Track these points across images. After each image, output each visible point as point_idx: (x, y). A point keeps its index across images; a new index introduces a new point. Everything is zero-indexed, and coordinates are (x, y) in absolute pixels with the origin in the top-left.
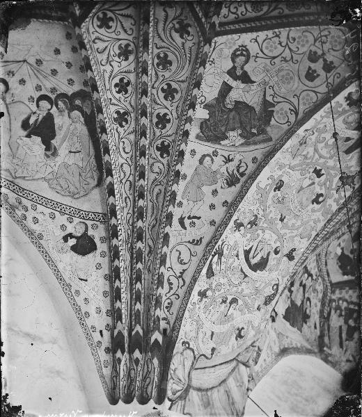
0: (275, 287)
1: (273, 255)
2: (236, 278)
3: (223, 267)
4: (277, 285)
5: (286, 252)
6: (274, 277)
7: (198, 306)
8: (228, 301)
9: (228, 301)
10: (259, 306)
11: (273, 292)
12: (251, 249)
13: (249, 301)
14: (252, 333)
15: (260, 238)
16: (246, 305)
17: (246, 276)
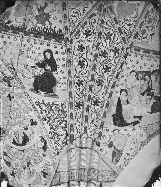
0: (42, 140)
1: (26, 132)
2: (21, 155)
3: (11, 157)
4: (43, 138)
7: (14, 180)
8: (26, 166)
9: (26, 166)
10: (43, 154)
11: (44, 143)
12: (14, 140)
14: (52, 167)
15: (13, 133)
17: (23, 150)
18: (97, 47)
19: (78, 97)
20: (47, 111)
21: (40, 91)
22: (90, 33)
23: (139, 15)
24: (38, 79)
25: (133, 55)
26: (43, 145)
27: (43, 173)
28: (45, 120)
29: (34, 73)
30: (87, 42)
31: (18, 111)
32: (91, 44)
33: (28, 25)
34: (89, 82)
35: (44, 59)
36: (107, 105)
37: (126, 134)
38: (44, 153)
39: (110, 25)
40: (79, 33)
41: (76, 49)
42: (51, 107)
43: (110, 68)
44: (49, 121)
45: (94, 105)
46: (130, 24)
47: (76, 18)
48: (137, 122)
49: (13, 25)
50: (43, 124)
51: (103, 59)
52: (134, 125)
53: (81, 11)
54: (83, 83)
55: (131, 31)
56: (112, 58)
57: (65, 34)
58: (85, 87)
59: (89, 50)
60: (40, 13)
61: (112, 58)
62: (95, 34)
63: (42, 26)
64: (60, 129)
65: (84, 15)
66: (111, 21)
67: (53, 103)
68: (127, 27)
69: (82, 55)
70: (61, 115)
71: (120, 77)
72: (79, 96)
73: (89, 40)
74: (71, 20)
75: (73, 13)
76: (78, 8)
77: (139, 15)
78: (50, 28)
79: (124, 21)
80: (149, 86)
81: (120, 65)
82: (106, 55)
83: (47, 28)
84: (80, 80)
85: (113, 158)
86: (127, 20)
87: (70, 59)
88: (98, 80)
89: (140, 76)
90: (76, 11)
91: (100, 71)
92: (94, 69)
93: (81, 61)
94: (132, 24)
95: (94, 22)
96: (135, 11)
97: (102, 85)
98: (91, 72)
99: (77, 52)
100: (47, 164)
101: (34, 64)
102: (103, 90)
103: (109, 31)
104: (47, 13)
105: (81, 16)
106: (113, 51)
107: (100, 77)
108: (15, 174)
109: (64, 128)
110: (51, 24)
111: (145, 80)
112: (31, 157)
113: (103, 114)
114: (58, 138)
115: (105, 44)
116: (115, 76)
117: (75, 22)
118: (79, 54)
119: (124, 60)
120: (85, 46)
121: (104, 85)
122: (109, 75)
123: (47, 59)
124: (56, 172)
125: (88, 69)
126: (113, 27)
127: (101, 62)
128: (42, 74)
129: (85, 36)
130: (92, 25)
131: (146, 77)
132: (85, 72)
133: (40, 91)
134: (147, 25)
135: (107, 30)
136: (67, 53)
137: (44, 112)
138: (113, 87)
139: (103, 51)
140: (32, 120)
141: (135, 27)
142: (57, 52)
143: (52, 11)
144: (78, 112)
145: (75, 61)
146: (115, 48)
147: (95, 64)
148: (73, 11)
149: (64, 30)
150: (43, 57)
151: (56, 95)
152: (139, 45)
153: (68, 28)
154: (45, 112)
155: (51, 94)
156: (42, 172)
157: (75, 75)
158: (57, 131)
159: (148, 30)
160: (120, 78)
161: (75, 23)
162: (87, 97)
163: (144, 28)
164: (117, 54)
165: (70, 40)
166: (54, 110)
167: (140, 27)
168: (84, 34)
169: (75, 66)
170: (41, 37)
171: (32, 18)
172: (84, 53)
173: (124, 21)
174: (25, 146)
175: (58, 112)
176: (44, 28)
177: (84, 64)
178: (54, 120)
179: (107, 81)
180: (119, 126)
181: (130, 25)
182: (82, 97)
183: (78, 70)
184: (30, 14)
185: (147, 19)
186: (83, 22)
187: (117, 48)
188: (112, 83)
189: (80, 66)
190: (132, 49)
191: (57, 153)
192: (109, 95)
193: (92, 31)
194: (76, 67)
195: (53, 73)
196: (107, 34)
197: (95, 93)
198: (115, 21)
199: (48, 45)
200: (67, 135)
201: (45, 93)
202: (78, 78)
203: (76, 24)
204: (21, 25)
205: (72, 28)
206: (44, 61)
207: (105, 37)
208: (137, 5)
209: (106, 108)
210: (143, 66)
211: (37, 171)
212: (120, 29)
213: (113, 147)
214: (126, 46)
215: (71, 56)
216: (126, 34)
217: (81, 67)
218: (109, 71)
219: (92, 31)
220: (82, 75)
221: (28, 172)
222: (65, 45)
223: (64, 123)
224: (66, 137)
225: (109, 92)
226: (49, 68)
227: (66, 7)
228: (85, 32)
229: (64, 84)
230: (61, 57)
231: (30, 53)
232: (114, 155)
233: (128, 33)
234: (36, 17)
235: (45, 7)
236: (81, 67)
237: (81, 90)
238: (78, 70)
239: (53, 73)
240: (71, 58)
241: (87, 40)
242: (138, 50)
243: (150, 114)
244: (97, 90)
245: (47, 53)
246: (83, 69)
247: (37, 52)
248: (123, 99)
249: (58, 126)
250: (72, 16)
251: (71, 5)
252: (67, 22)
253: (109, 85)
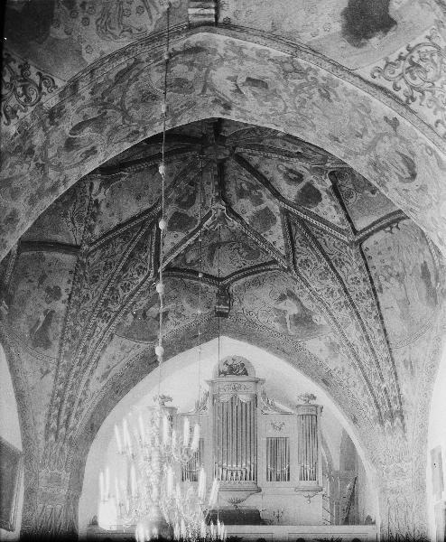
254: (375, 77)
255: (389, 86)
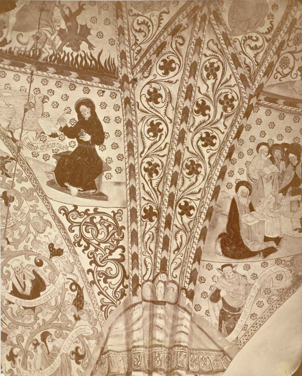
0: (74, 287)
1: (40, 270)
4: (75, 283)
5: (47, 254)
6: (62, 281)
7: (15, 370)
8: (40, 341)
9: (40, 341)
10: (75, 316)
11: (76, 293)
12: (14, 286)
13: (60, 322)
14: (93, 342)
15: (12, 272)
16: (60, 327)
17: (33, 308)
18: (187, 94)
19: (147, 197)
20: (84, 227)
21: (68, 185)
22: (173, 65)
23: (275, 27)
24: (64, 161)
25: (262, 110)
26: (74, 298)
27: (74, 355)
28: (80, 246)
29: (56, 148)
30: (168, 85)
31: (23, 228)
32: (174, 89)
33: (43, 49)
34: (171, 168)
35: (77, 120)
36: (209, 215)
37: (248, 274)
38: (77, 314)
39: (215, 48)
40: (151, 66)
41: (144, 99)
42: (92, 219)
43: (214, 137)
44: (86, 248)
45: (181, 214)
46: (256, 46)
47: (143, 34)
48: (271, 250)
49: (13, 49)
50: (76, 253)
51: (199, 118)
52: (265, 256)
53: (155, 20)
54: (157, 168)
55: (259, 61)
56: (218, 116)
57: (121, 68)
58: (162, 178)
59: (171, 101)
60: (69, 24)
61: (218, 116)
62: (183, 69)
63: (71, 51)
64: (110, 265)
65: (160, 29)
66: (216, 41)
67: (95, 210)
68: (251, 53)
69: (156, 111)
70: (113, 234)
71: (235, 156)
72: (150, 196)
73: (170, 80)
74: (132, 38)
75: (138, 24)
76: (148, 15)
77: (275, 27)
78: (89, 55)
79: (245, 41)
80: (296, 175)
81: (236, 132)
82: (207, 112)
83: (83, 55)
84: (153, 163)
85: (220, 323)
86: (250, 38)
87: (131, 120)
88: (189, 163)
89: (277, 153)
90: (144, 21)
91: (195, 144)
92: (181, 139)
93: (155, 123)
94: (260, 47)
95: (181, 42)
96: (266, 19)
97: (198, 173)
98: (174, 147)
99: (146, 104)
100: (82, 336)
101: (56, 129)
102: (201, 184)
103: (211, 61)
104: (84, 24)
105: (154, 31)
106: (221, 102)
107: (195, 156)
108: (16, 356)
109: (119, 261)
110: (91, 46)
111: (288, 162)
112: (50, 323)
113: (199, 233)
114: (105, 282)
115: (203, 89)
116: (225, 155)
117: (141, 43)
118: (150, 109)
119: (244, 122)
120: (162, 92)
121: (203, 173)
122: (211, 152)
123: (84, 118)
124: (102, 353)
125: (168, 140)
126: (220, 53)
127: (196, 124)
128: (72, 150)
129: (163, 71)
130: (176, 48)
131: (291, 155)
132: (163, 146)
133: (68, 185)
134: (293, 49)
135: (209, 59)
136: (125, 107)
137: (76, 229)
138: (222, 176)
139: (200, 102)
140: (51, 246)
141: (266, 53)
142: (104, 106)
143: (94, 20)
144: (147, 229)
145: (141, 124)
146: (226, 97)
147: (183, 129)
148: (138, 20)
149: (119, 59)
150: (75, 115)
151: (101, 194)
152: (275, 91)
153: (128, 54)
154: (80, 229)
155: (92, 191)
156: (73, 353)
157: (142, 153)
158: (104, 269)
159: (294, 58)
160: (237, 158)
161: (141, 45)
162: (167, 199)
163: (285, 55)
164: (229, 109)
165: (130, 80)
166: (98, 226)
167: (278, 53)
168: (161, 68)
169: (141, 133)
170: (71, 74)
171: (52, 35)
172: (161, 106)
173: (245, 41)
174: (38, 299)
175: (105, 229)
176: (78, 55)
177: (161, 130)
178: (99, 245)
179: (209, 164)
180: (233, 257)
181: (256, 48)
182: (156, 198)
183: (148, 143)
184: (47, 26)
185: (292, 36)
186: (158, 43)
187: (230, 97)
188: (219, 168)
189: (151, 134)
190: (262, 97)
191: (103, 313)
192: (212, 192)
193: (177, 61)
194: (144, 136)
195: (97, 147)
196: (208, 66)
197: (183, 189)
198: (225, 41)
199: (87, 90)
200: (125, 276)
201: (79, 190)
202: (149, 159)
203: (145, 46)
204: (28, 49)
205: (135, 55)
206: (78, 123)
207: (205, 73)
208: (270, 7)
209: (207, 221)
210: (283, 132)
211: (62, 351)
212: (234, 57)
213: (220, 302)
214: (249, 91)
215: (133, 112)
216: (248, 66)
217: (155, 135)
218: (213, 145)
219: (177, 61)
220: (156, 153)
221: (43, 354)
222: (120, 90)
223: (119, 251)
224: (122, 282)
225: (213, 187)
226: (87, 138)
227: (122, 11)
228: (162, 64)
229: (119, 170)
230: (113, 114)
231: (48, 107)
232: (223, 316)
233: (252, 65)
234: (61, 33)
235: (78, 12)
236: (153, 137)
237: (154, 183)
238: (148, 143)
239: (97, 147)
240: (134, 118)
241: (167, 80)
242: (273, 99)
243: (299, 232)
244: (187, 183)
245: (83, 108)
246: (158, 139)
247: (63, 105)
248: (243, 202)
249: (107, 257)
250: (136, 30)
251: (133, 9)
252: (124, 43)
253: (213, 173)
254: (61, 213)
255: (67, 225)
